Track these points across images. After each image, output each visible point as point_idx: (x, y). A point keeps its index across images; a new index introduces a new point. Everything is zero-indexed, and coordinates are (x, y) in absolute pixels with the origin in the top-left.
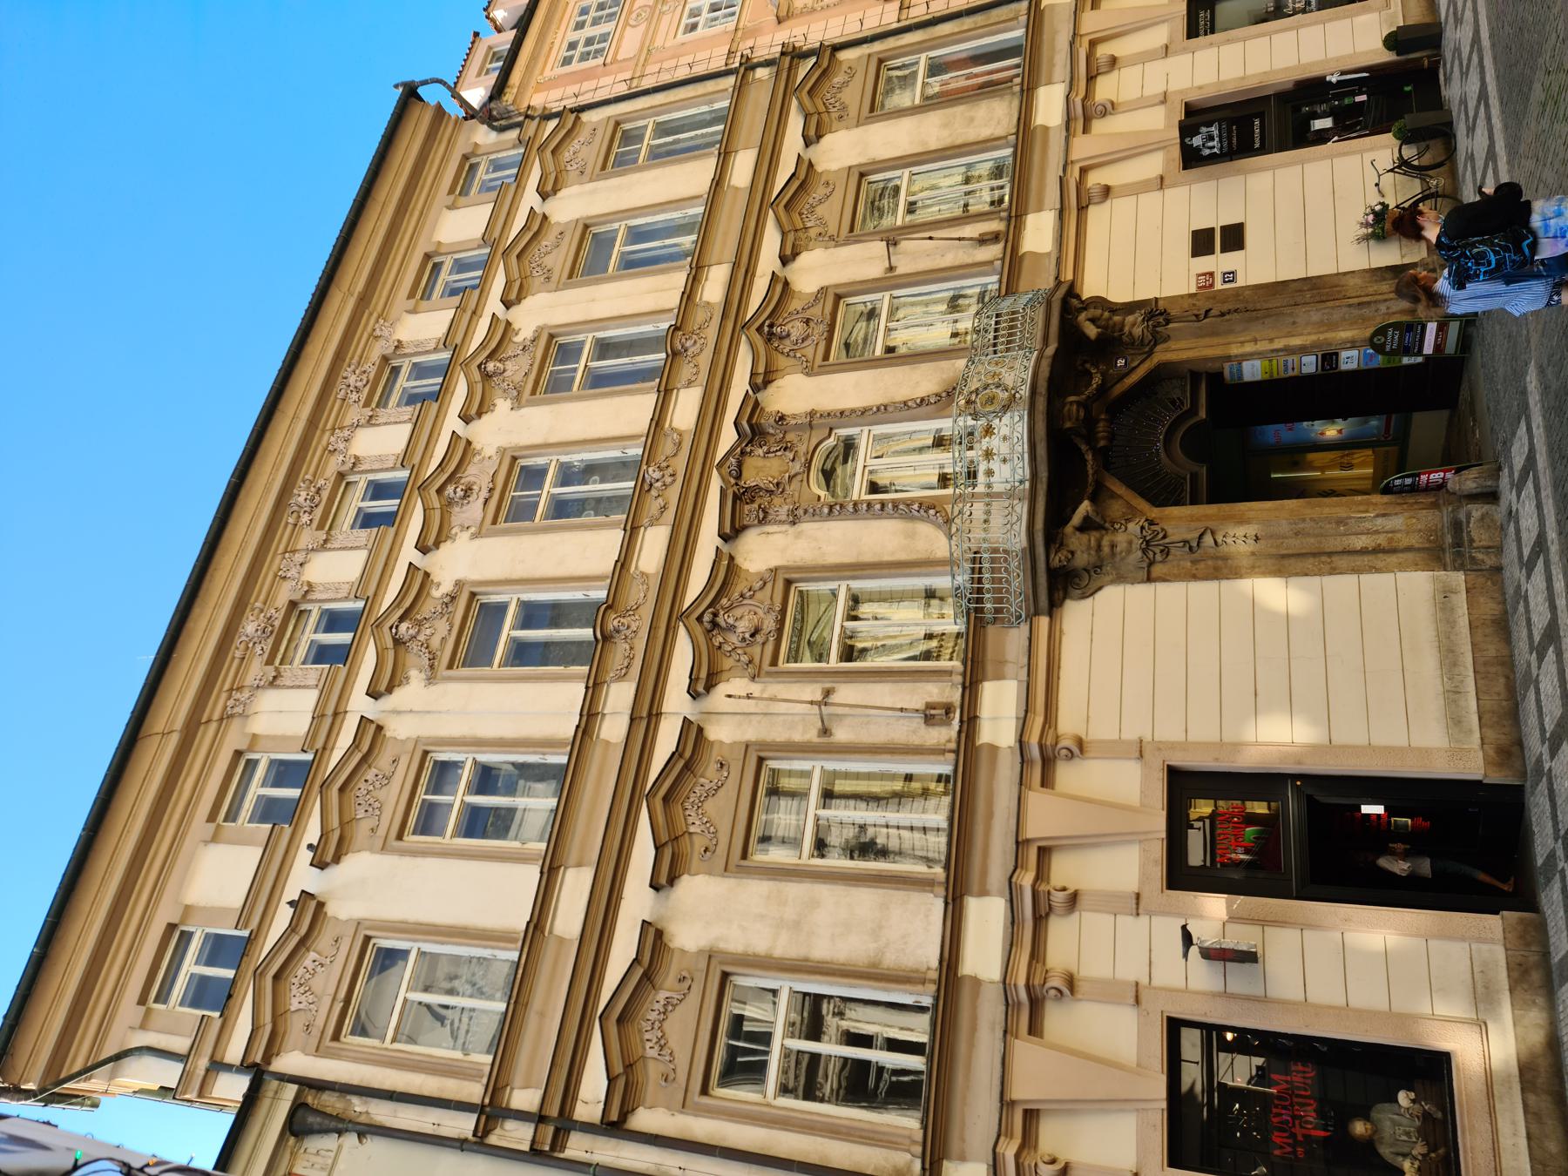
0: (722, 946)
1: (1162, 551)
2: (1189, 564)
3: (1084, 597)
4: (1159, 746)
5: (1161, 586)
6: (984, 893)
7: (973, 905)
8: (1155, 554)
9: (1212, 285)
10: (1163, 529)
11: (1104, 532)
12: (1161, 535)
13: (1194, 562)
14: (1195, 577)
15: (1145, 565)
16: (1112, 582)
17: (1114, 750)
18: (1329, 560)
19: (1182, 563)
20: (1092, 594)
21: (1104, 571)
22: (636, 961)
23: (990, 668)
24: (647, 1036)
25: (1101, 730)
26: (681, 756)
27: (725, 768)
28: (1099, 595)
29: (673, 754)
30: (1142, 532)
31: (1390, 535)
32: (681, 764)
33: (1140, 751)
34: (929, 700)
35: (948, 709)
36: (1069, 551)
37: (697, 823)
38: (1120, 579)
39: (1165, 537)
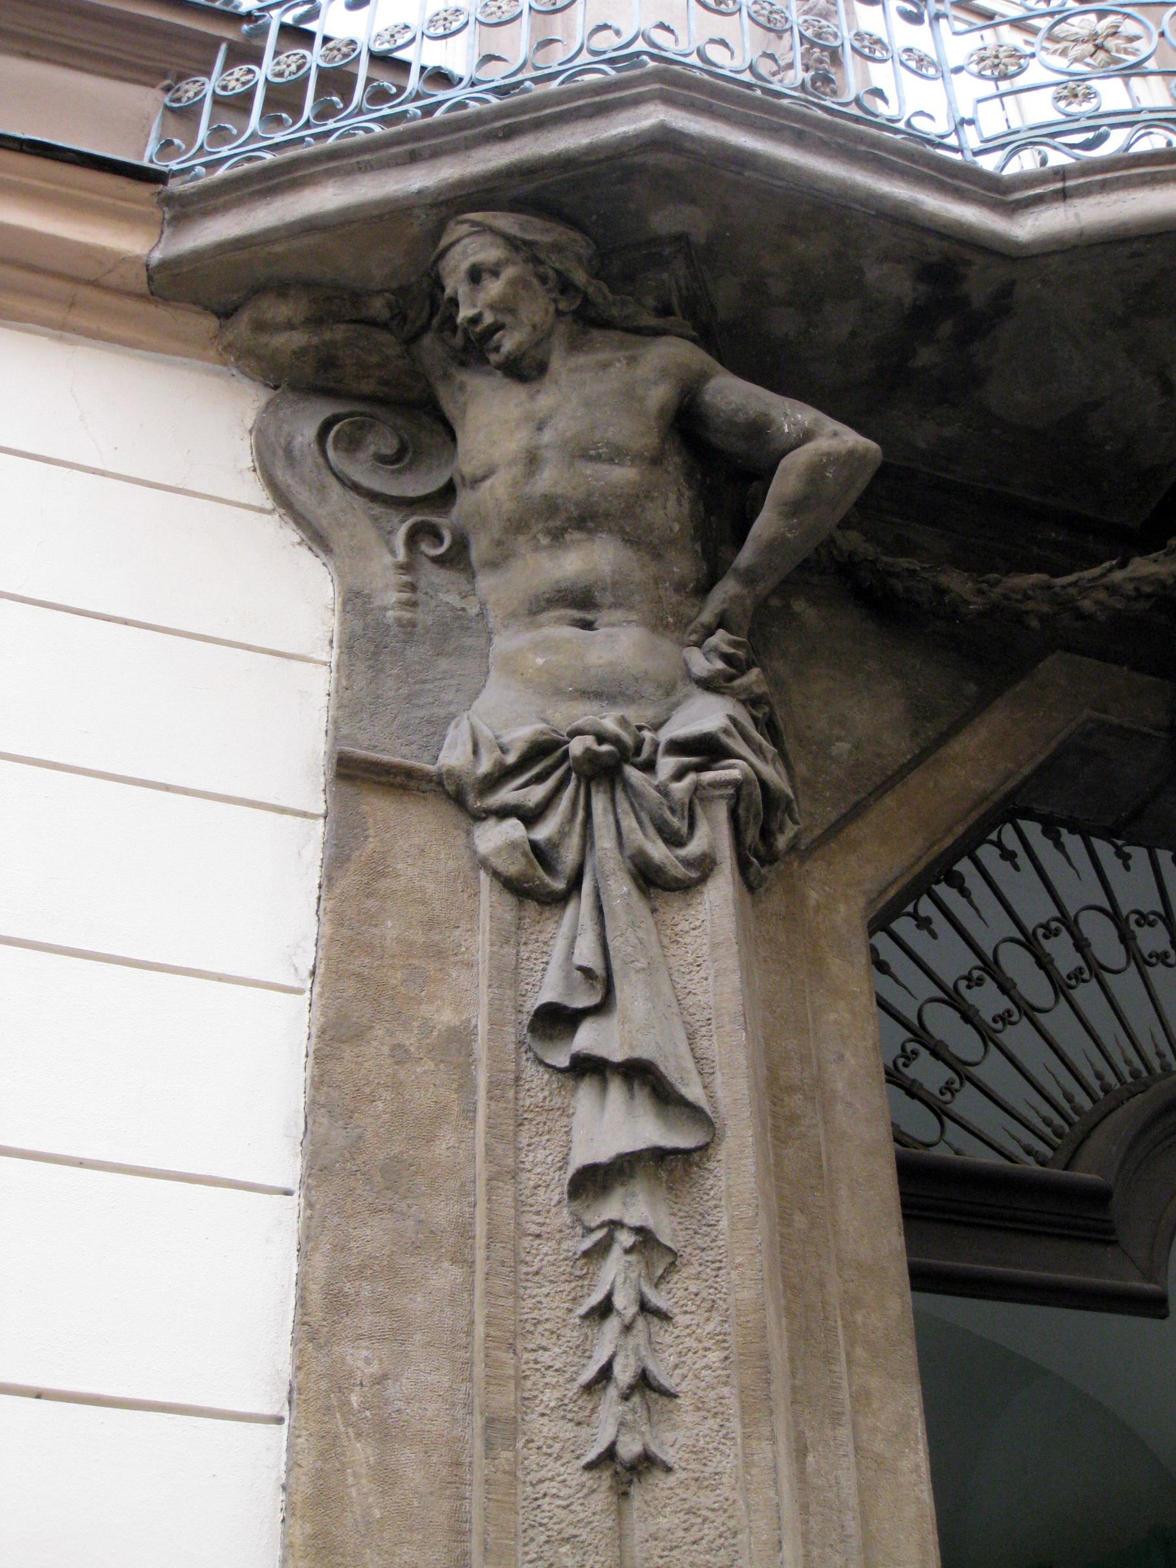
1: (542, 854)
2: (447, 1017)
8: (531, 817)
10: (705, 866)
21: (432, 576)
30: (678, 747)
36: (542, 339)
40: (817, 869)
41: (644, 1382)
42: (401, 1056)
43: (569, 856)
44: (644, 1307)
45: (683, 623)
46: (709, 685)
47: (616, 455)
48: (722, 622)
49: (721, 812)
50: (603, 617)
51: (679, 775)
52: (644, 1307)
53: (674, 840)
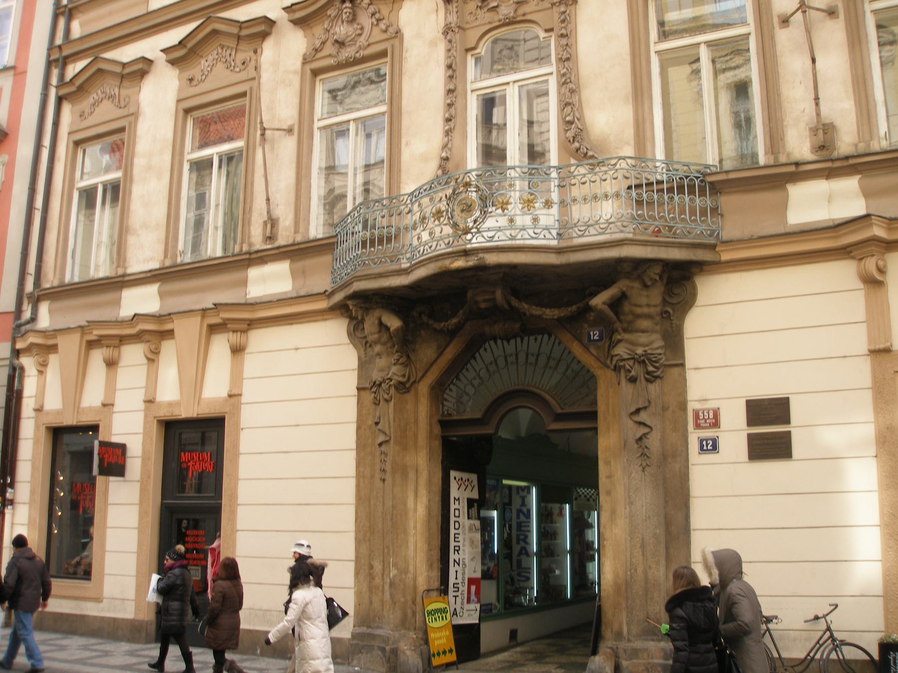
0: (141, 119)
3: (349, 334)
4: (237, 409)
5: (354, 401)
6: (162, 295)
7: (152, 289)
9: (698, 426)
10: (391, 397)
11: (389, 345)
12: (386, 396)
13: (370, 427)
14: (358, 428)
15: (367, 385)
16: (359, 359)
17: (237, 376)
18: (367, 539)
19: (371, 416)
20: (351, 342)
21: (369, 350)
22: (124, 65)
23: (300, 264)
24: (99, 92)
25: (252, 363)
26: (241, 28)
27: (243, 67)
28: (351, 346)
29: (238, 22)
31: (381, 588)
32: (235, 30)
33: (234, 396)
34: (281, 220)
35: (271, 238)
37: (206, 64)
38: (363, 366)
39: (387, 401)
40: (421, 383)
41: (384, 470)
42: (365, 430)
43: (378, 399)
44: (384, 460)
45: (392, 353)
46: (395, 364)
47: (374, 333)
48: (397, 352)
49: (393, 388)
50: (382, 356)
51: (388, 383)
52: (384, 460)
53: (388, 394)
